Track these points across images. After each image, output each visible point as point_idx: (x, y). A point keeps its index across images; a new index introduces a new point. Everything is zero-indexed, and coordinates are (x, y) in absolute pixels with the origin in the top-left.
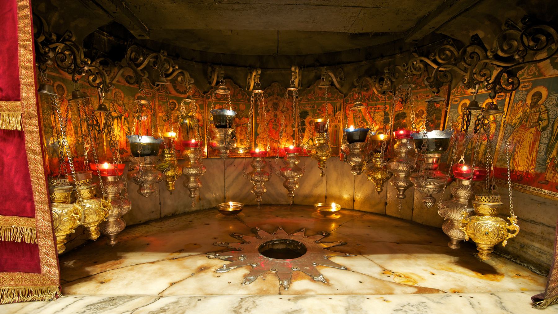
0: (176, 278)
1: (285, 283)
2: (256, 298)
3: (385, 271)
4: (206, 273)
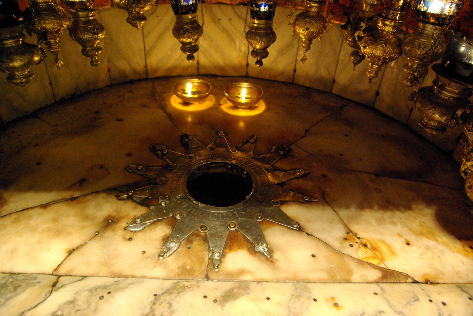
1: (216, 256)
2: (173, 296)
3: (350, 235)
4: (114, 230)
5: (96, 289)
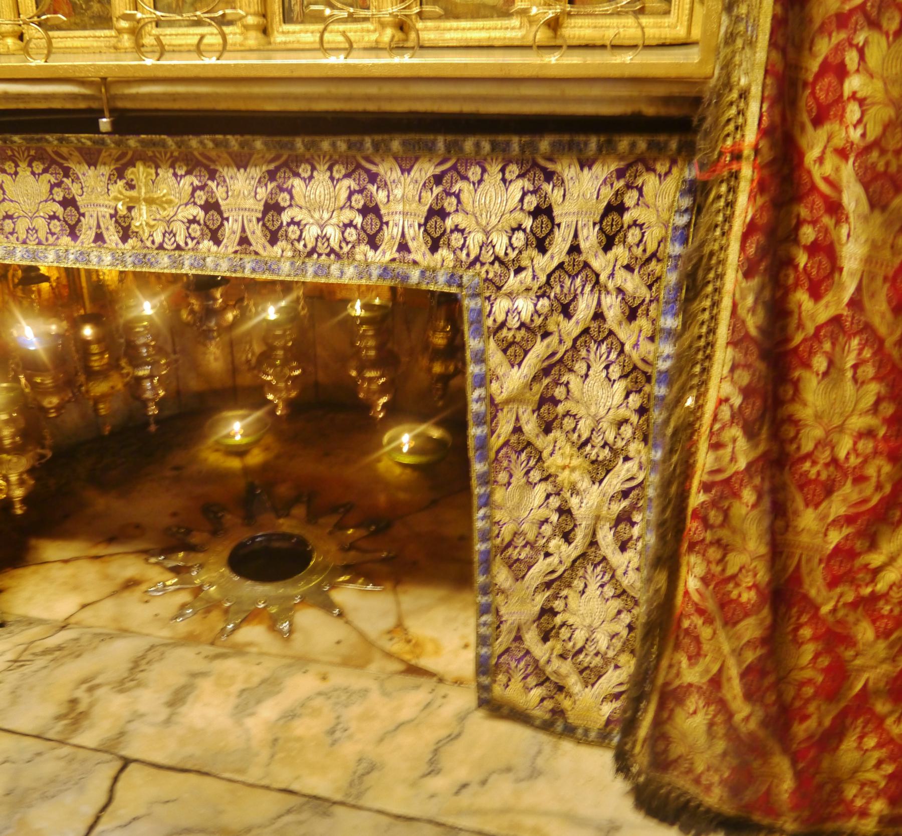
0: (91, 598)
5: (101, 634)
